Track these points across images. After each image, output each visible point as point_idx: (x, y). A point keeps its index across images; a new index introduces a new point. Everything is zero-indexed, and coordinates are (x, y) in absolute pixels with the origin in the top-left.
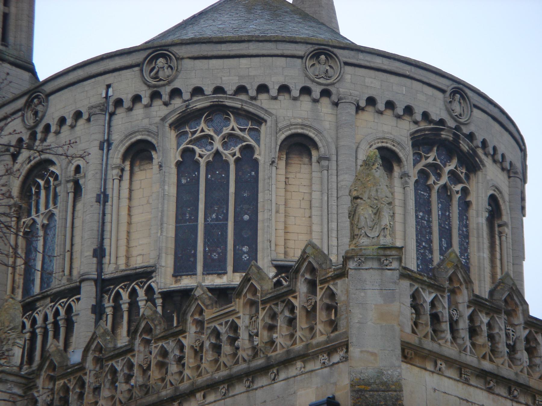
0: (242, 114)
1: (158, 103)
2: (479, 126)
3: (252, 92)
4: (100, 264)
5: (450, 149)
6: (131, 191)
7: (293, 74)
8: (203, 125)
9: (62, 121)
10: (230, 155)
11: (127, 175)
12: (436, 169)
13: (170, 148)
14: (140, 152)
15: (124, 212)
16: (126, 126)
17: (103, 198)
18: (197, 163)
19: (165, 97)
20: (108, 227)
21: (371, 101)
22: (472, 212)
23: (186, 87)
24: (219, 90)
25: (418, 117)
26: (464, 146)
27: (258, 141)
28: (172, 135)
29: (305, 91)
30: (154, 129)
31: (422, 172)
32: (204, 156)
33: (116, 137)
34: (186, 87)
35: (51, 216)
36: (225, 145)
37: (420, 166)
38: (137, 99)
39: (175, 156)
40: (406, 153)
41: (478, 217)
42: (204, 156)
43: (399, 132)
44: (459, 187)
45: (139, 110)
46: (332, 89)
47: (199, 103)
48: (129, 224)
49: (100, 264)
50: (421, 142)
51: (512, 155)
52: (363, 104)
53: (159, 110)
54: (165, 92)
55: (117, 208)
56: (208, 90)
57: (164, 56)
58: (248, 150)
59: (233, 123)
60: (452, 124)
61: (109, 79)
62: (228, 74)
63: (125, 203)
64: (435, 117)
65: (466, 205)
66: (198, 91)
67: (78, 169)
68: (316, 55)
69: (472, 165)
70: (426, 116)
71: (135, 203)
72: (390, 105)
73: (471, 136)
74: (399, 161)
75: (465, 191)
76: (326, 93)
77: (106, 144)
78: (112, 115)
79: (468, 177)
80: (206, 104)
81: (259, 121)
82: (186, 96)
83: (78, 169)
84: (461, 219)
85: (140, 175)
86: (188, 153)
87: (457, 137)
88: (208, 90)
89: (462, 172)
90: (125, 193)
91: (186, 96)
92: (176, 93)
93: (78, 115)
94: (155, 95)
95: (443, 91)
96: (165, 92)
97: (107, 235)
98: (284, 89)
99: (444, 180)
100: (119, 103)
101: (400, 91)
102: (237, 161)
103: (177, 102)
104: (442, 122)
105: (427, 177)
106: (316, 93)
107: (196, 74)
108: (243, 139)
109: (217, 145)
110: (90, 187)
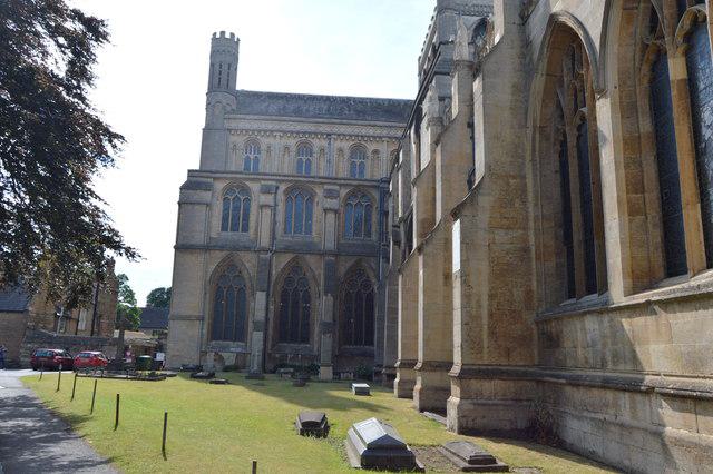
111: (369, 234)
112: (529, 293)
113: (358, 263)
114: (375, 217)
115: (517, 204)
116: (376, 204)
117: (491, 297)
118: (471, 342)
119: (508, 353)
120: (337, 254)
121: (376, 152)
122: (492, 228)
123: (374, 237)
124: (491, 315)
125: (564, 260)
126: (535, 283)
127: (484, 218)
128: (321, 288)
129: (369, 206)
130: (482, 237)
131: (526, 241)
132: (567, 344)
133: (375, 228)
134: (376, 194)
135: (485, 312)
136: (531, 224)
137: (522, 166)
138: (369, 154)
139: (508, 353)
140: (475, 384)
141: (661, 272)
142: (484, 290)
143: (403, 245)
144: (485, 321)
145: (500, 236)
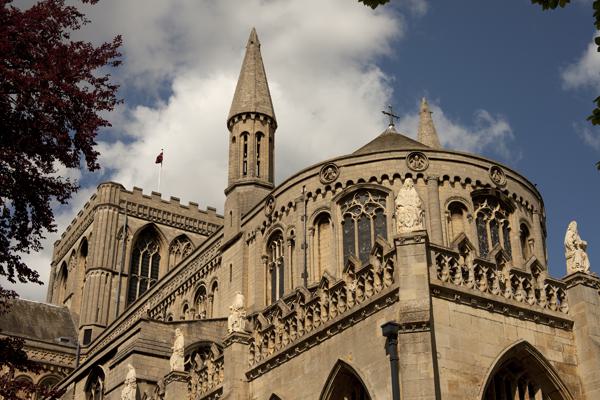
0: (375, 192)
1: (329, 192)
3: (379, 180)
4: (306, 281)
5: (493, 201)
6: (319, 241)
7: (401, 167)
8: (354, 200)
9: (283, 209)
11: (316, 232)
12: (487, 211)
13: (337, 214)
14: (323, 218)
15: (316, 252)
16: (312, 207)
17: (305, 246)
18: (353, 221)
19: (333, 188)
20: (308, 261)
21: (446, 178)
22: (511, 234)
23: (343, 180)
24: (361, 180)
25: (474, 184)
26: (503, 198)
27: (384, 205)
28: (339, 207)
29: (408, 175)
30: (328, 205)
31: (479, 214)
33: (309, 213)
34: (343, 180)
35: (281, 260)
36: (367, 209)
37: (477, 211)
38: (319, 191)
39: (341, 219)
40: (470, 205)
41: (515, 236)
43: (465, 193)
44: (502, 221)
45: (320, 196)
46: (423, 173)
48: (320, 258)
49: (306, 281)
50: (477, 198)
52: (441, 179)
54: (333, 186)
55: (313, 250)
56: (355, 182)
57: (331, 167)
59: (371, 197)
60: (494, 186)
61: (304, 183)
62: (364, 172)
63: (316, 247)
64: (484, 183)
65: (507, 230)
66: (350, 183)
67: (292, 233)
68: (412, 156)
70: (478, 183)
71: (321, 247)
72: (457, 179)
73: (506, 192)
74: (466, 209)
75: (506, 223)
76: (420, 176)
78: (307, 201)
79: (507, 215)
80: (356, 189)
81: (385, 195)
82: (344, 186)
83: (292, 233)
84: (505, 238)
85: (323, 232)
86: (347, 216)
88: (355, 182)
90: (316, 242)
91: (344, 186)
92: (339, 185)
93: (290, 205)
94: (328, 188)
95: (487, 169)
96: (333, 186)
97: (308, 265)
98: (397, 176)
99: (493, 217)
100: (310, 195)
102: (374, 217)
103: (340, 190)
104: (488, 185)
105: (483, 216)
106: (415, 177)
107: (347, 175)
108: (377, 205)
109: (363, 210)
110: (299, 241)
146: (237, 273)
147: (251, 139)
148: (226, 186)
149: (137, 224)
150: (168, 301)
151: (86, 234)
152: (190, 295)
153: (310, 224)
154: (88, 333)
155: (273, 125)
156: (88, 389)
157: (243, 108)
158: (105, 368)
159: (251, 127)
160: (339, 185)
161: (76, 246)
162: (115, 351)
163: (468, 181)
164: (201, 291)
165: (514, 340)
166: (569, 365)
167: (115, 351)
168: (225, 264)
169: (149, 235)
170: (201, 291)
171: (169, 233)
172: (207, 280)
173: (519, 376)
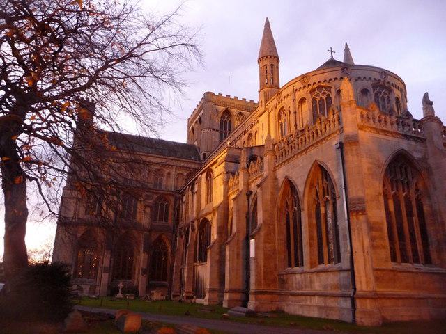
2: (390, 79)
9: (285, 97)
10: (324, 97)
14: (302, 101)
16: (299, 95)
21: (359, 78)
31: (376, 94)
32: (318, 99)
38: (300, 88)
40: (371, 89)
42: (318, 99)
45: (301, 91)
47: (315, 86)
50: (375, 87)
51: (401, 86)
53: (306, 89)
58: (328, 95)
66: (314, 83)
69: (390, 90)
70: (375, 79)
73: (388, 83)
75: (389, 97)
77: (294, 100)
86: (314, 99)
87: (384, 84)
89: (387, 92)
93: (288, 95)
94: (305, 86)
101: (367, 74)
103: (310, 87)
104: (380, 80)
110: (292, 111)
111: (166, 220)
112: (275, 265)
113: (160, 236)
114: (171, 211)
115: (272, 234)
116: (172, 203)
117: (264, 266)
118: (258, 282)
119: (269, 285)
120: (150, 230)
121: (169, 173)
122: (265, 242)
123: (170, 222)
124: (264, 272)
125: (287, 255)
126: (277, 262)
127: (262, 239)
128: (142, 248)
129: (168, 206)
130: (262, 245)
131: (275, 247)
132: (290, 282)
133: (170, 217)
134: (172, 199)
135: (262, 271)
136: (277, 241)
137: (274, 221)
138: (165, 174)
139: (269, 285)
140: (260, 296)
141: (317, 263)
142: (262, 264)
143: (196, 231)
144: (262, 274)
145: (267, 245)
146: (266, 126)
147: (269, 68)
148: (258, 89)
149: (221, 109)
150: (236, 140)
151: (201, 114)
152: (246, 135)
153: (297, 103)
154: (204, 155)
155: (278, 60)
156: (206, 178)
157: (265, 54)
158: (213, 168)
159: (267, 62)
160: (309, 85)
161: (197, 119)
162: (216, 161)
163: (370, 78)
164: (250, 135)
165: (397, 148)
166: (424, 159)
167: (216, 161)
168: (260, 123)
169: (227, 112)
170: (250, 135)
171: (234, 111)
172: (254, 129)
173: (399, 165)
